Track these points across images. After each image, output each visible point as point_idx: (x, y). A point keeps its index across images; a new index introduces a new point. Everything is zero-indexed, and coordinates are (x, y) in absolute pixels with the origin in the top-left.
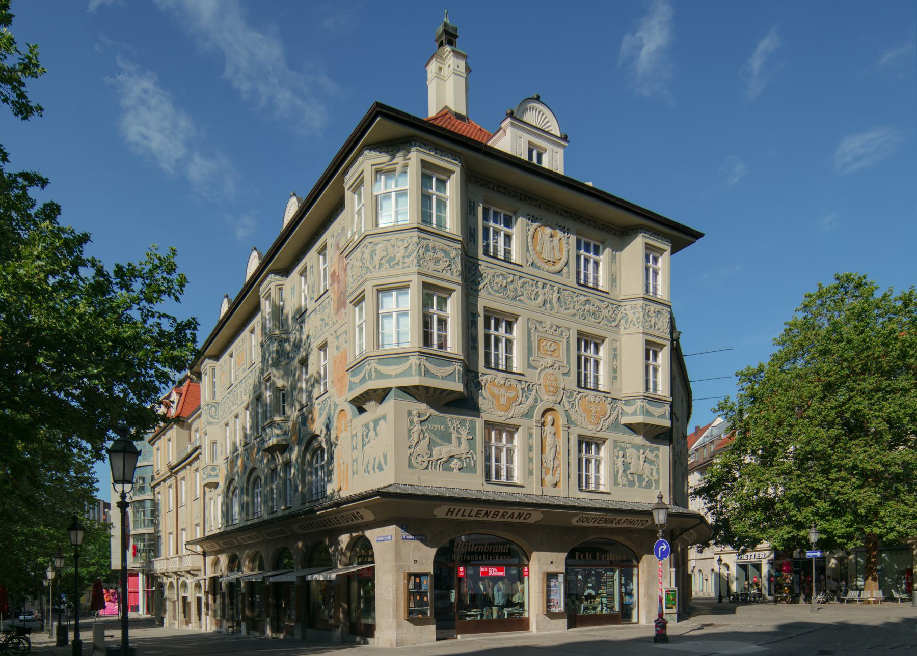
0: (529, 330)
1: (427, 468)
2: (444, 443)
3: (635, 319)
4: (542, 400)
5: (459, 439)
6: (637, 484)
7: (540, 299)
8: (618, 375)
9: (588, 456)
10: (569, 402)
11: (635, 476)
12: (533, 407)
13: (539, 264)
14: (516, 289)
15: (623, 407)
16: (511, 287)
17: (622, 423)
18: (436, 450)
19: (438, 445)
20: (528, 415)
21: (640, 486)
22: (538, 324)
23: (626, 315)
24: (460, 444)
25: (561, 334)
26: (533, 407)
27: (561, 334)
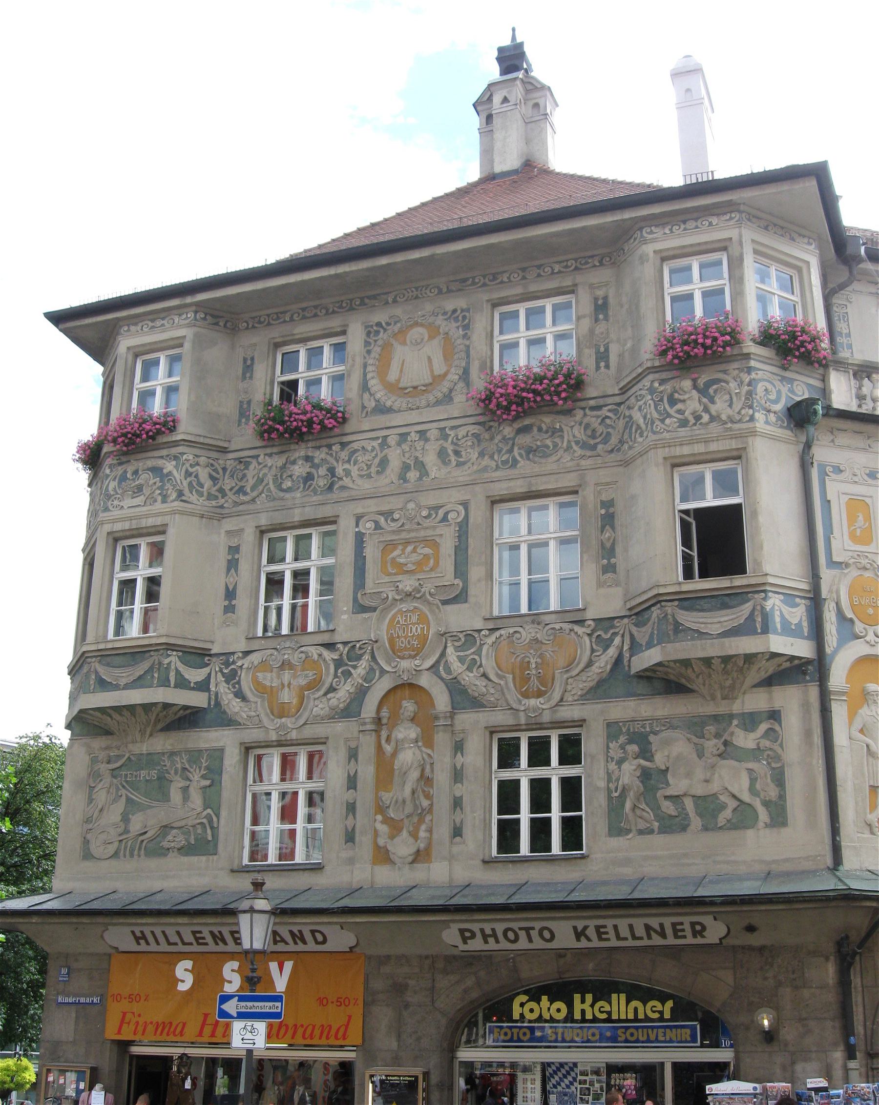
0: (360, 538)
1: (116, 855)
2: (155, 803)
3: (641, 421)
4: (383, 672)
5: (185, 790)
6: (696, 822)
7: (395, 463)
8: (619, 560)
9: (540, 772)
10: (461, 660)
11: (689, 803)
12: (361, 693)
13: (389, 403)
14: (332, 471)
15: (634, 630)
16: (322, 471)
17: (633, 671)
18: (136, 825)
19: (141, 808)
20: (350, 711)
21: (706, 829)
22: (382, 520)
23: (630, 417)
24: (186, 797)
25: (445, 519)
26: (361, 693)
27: (445, 519)
